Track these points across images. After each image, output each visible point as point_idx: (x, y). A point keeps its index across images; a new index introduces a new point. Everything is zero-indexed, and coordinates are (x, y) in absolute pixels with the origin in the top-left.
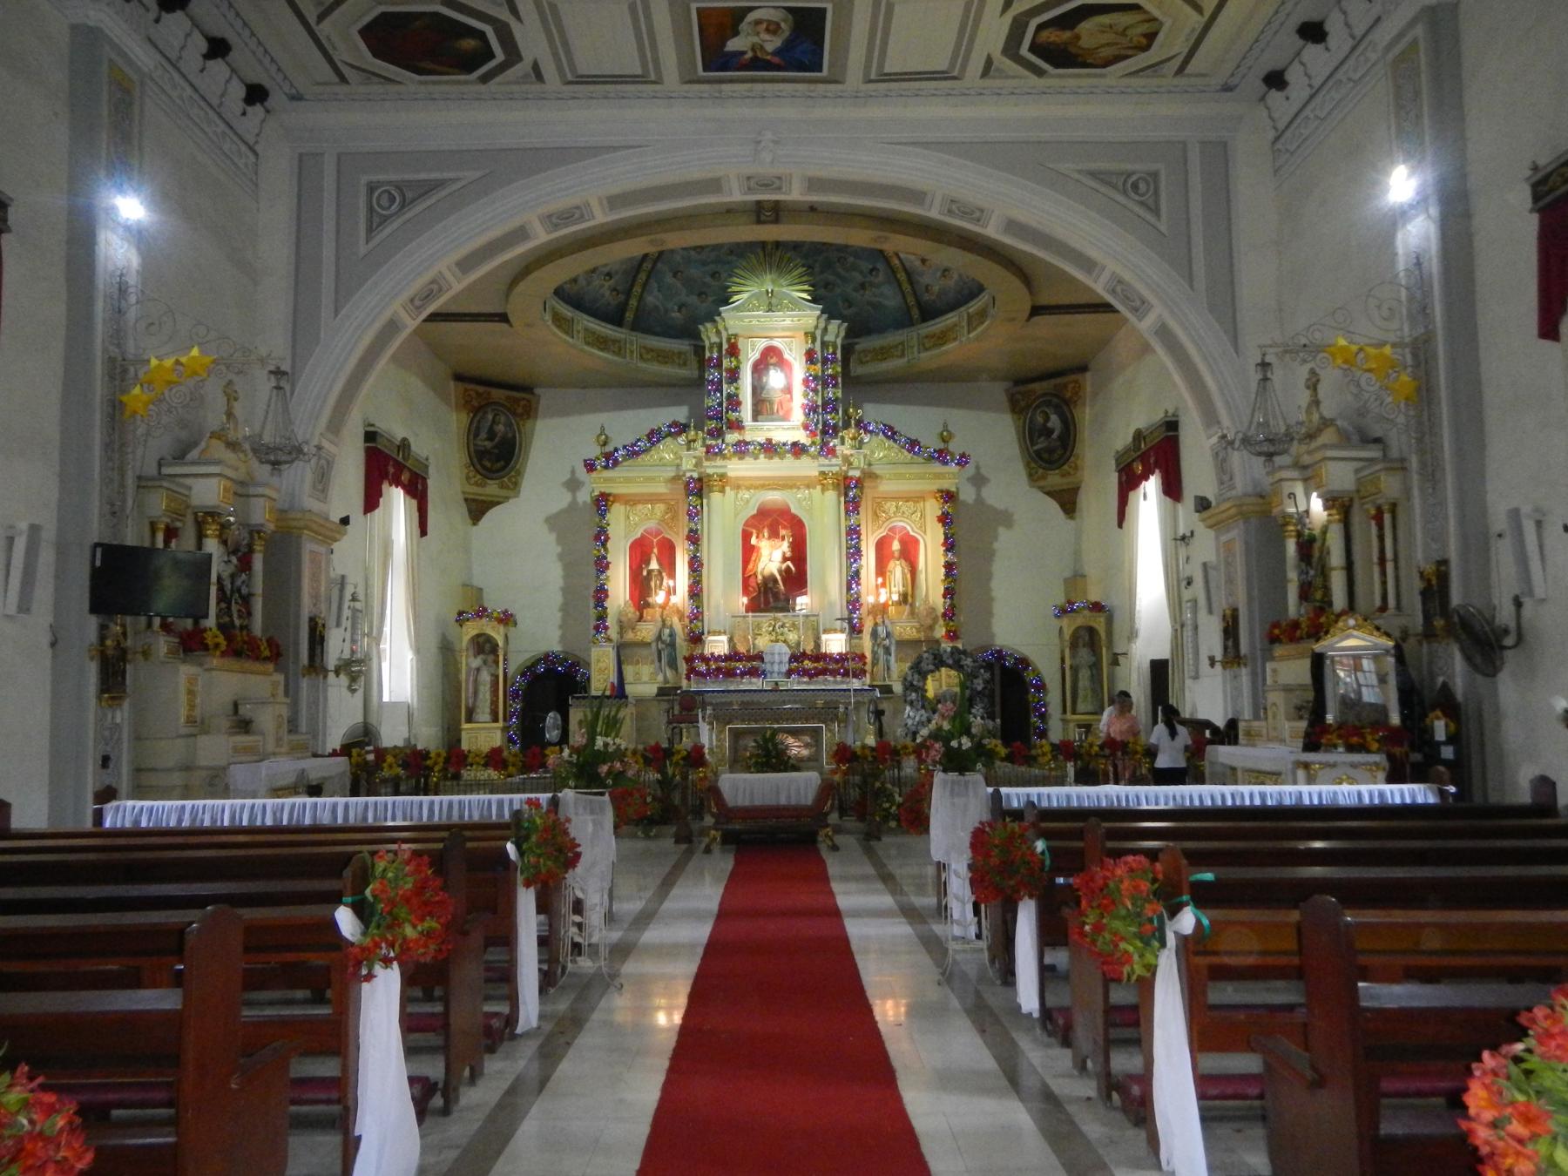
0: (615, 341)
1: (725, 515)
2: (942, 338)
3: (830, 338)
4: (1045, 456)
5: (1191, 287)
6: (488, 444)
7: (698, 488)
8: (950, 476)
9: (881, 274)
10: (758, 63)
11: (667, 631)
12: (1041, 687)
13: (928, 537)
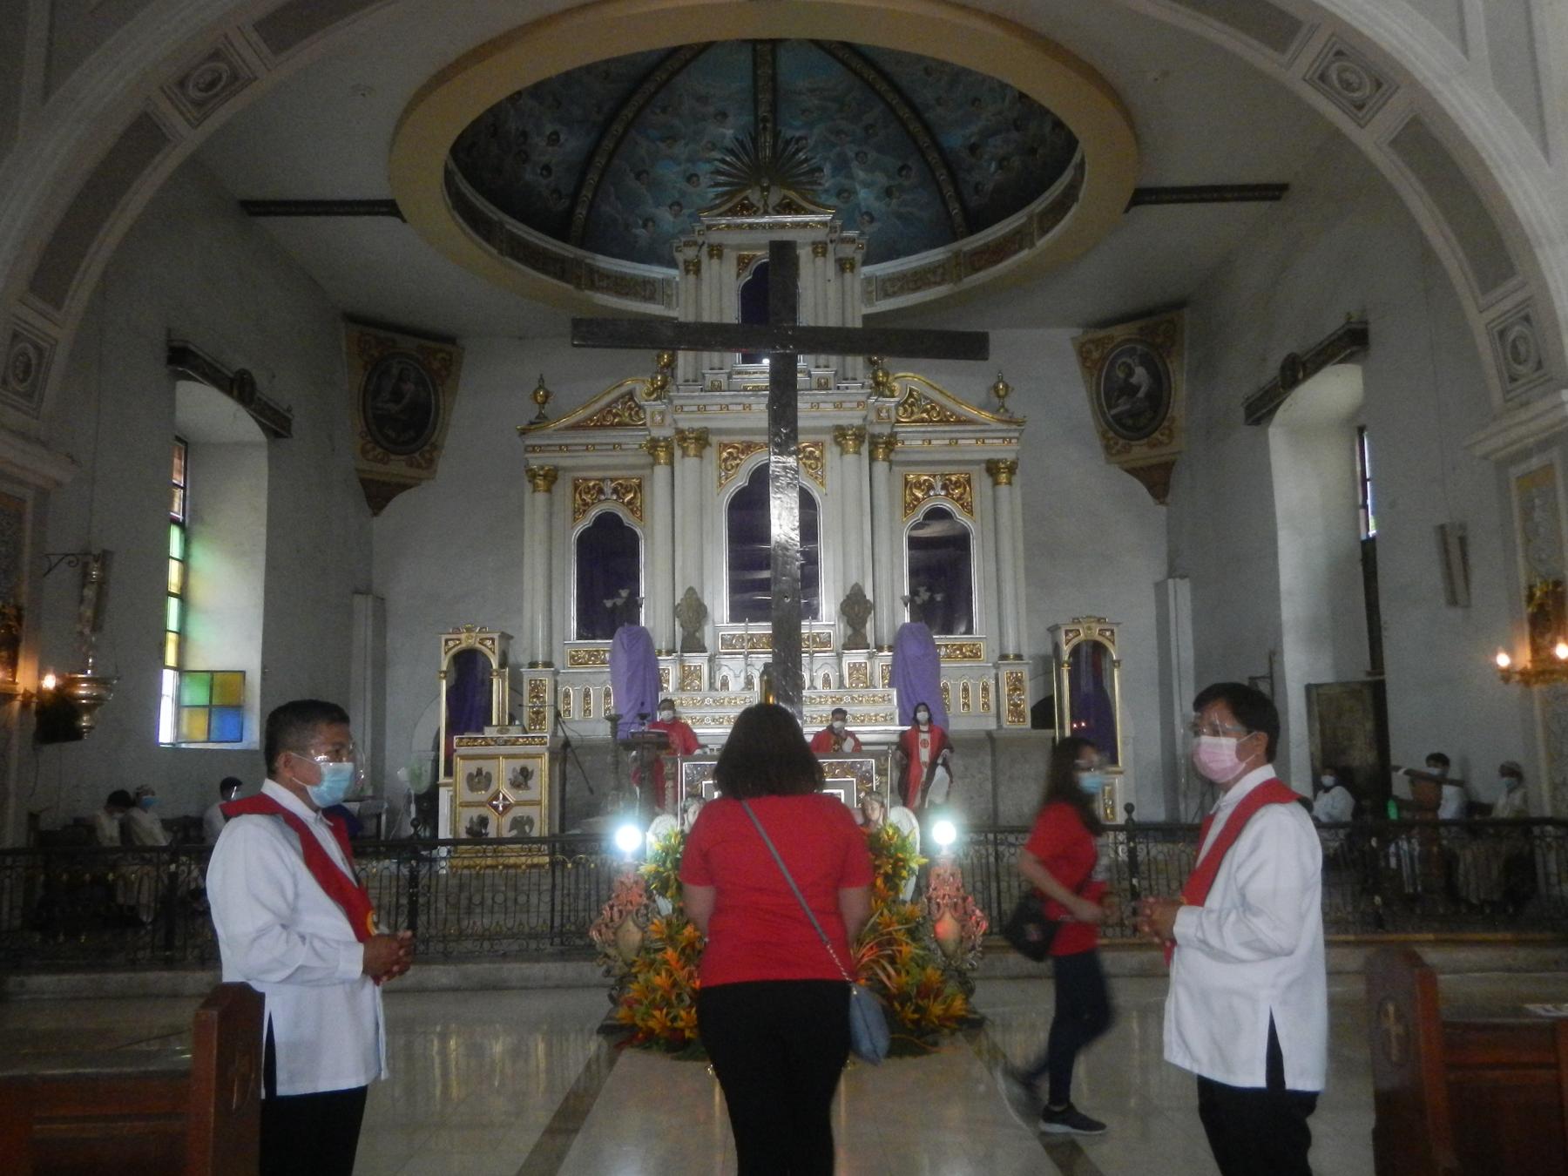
2: (997, 252)
4: (1130, 422)
5: (1466, 52)
6: (394, 408)
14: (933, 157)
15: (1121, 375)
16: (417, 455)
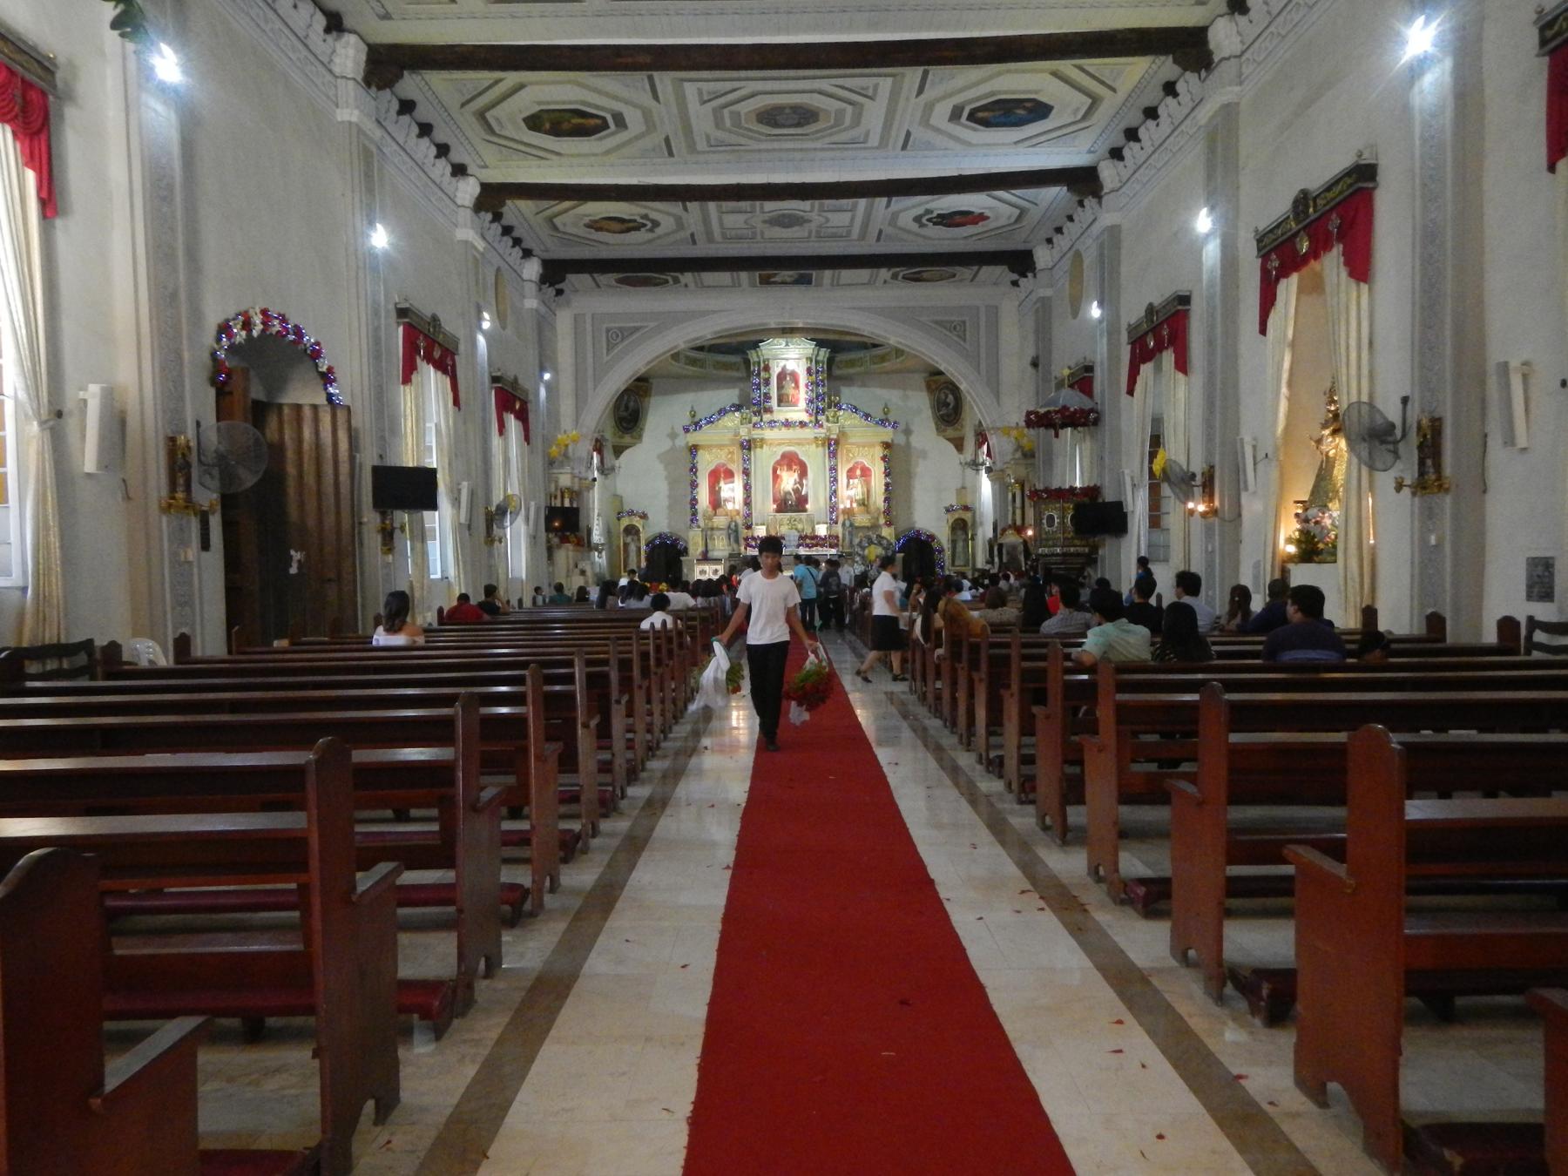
1: (764, 459)
7: (748, 446)
8: (887, 434)
10: (784, 283)
12: (941, 551)
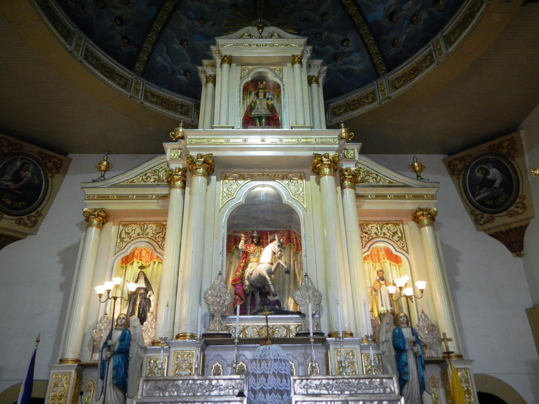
0: (121, 77)
2: (415, 71)
3: (314, 72)
4: (490, 203)
6: (12, 185)
9: (351, 43)
11: (117, 334)
13: (411, 256)
14: (364, 30)
15: (481, 176)
16: (25, 217)
